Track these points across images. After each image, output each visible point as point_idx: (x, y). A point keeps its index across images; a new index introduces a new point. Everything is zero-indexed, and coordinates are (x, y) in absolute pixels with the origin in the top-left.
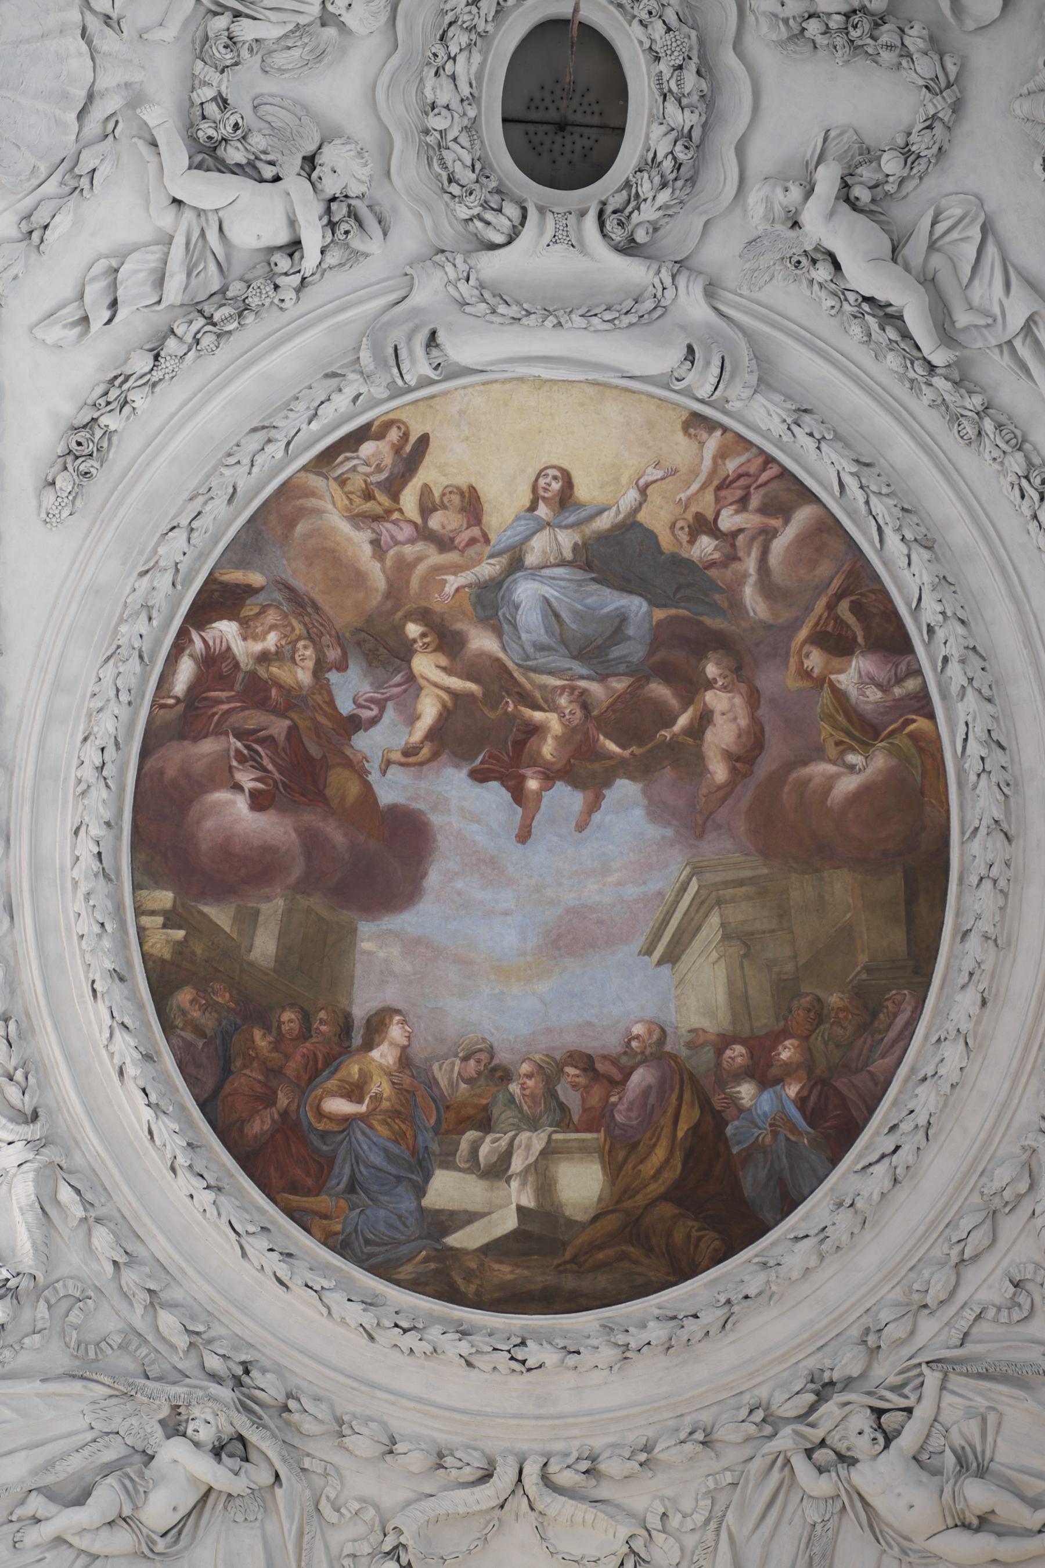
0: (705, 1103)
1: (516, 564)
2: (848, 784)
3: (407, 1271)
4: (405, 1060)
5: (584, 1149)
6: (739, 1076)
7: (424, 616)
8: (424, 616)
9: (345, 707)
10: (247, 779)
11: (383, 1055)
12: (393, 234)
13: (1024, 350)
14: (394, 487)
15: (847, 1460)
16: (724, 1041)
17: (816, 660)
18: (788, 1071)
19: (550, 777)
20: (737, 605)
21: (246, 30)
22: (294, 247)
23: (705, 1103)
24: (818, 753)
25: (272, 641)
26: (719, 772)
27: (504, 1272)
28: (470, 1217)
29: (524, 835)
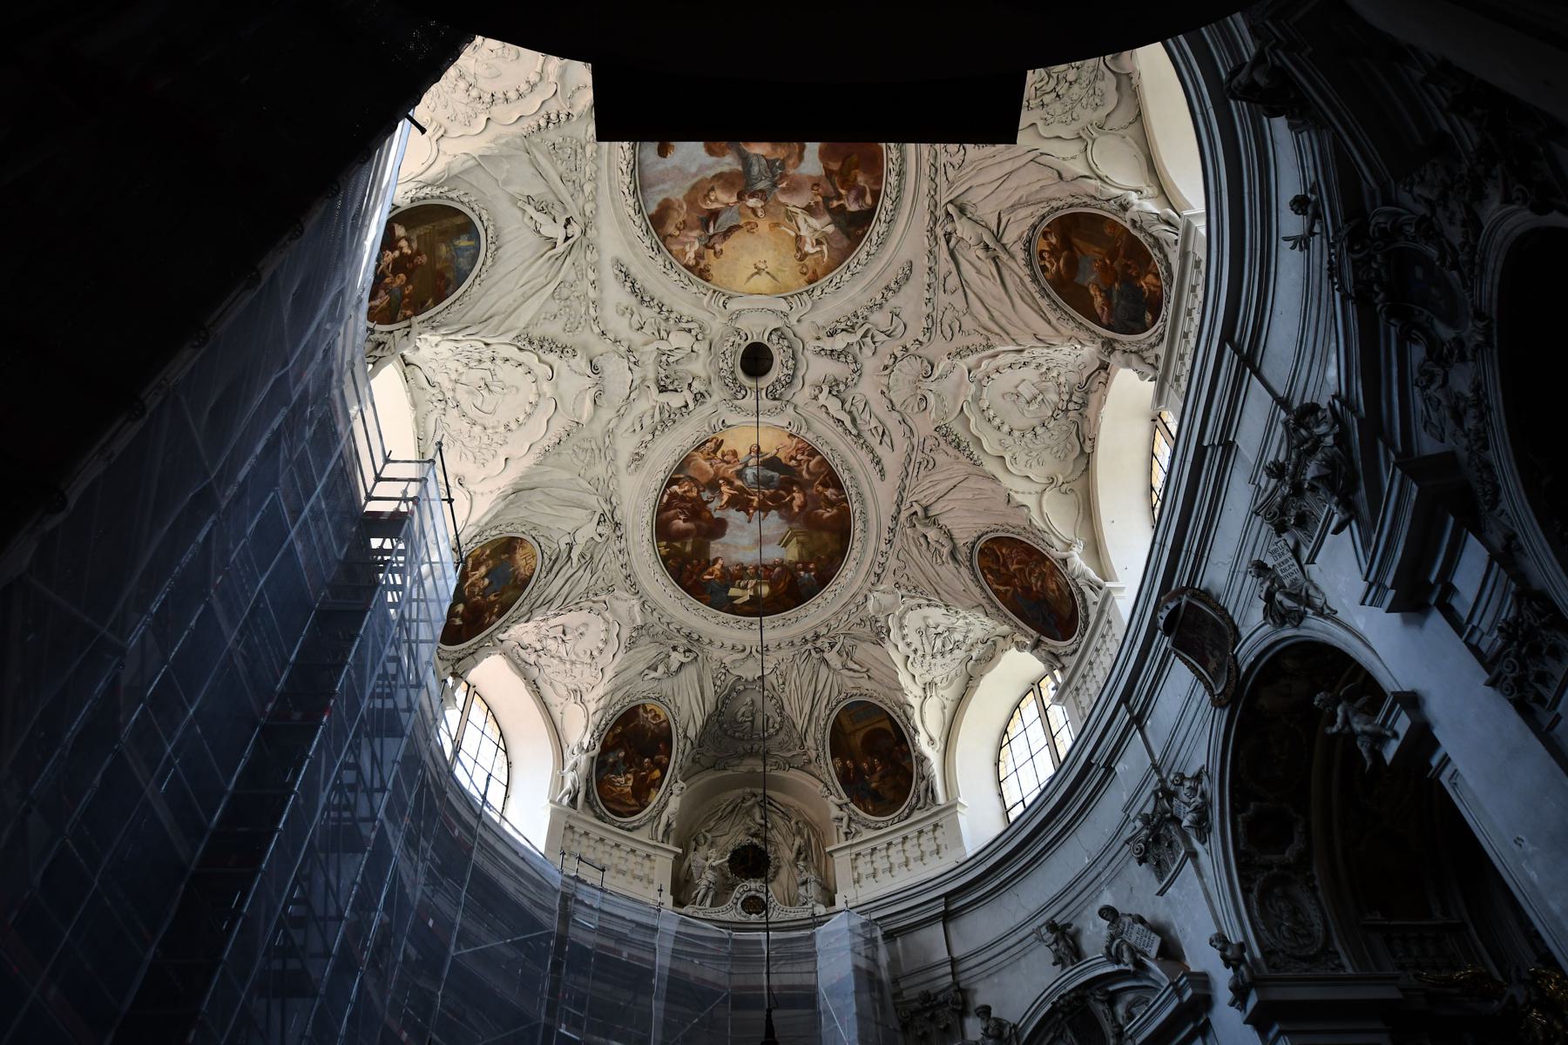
0: (792, 575)
1: (746, 465)
2: (827, 515)
3: (725, 609)
4: (722, 566)
5: (765, 583)
6: (801, 570)
7: (723, 478)
8: (723, 478)
9: (705, 499)
10: (682, 517)
11: (718, 566)
12: (713, 397)
13: (874, 432)
14: (715, 452)
15: (823, 651)
16: (797, 563)
17: (820, 488)
18: (811, 570)
19: (755, 509)
20: (801, 476)
21: (671, 359)
22: (686, 406)
23: (792, 575)
24: (821, 508)
25: (686, 488)
26: (797, 510)
27: (747, 608)
28: (739, 597)
29: (749, 522)
